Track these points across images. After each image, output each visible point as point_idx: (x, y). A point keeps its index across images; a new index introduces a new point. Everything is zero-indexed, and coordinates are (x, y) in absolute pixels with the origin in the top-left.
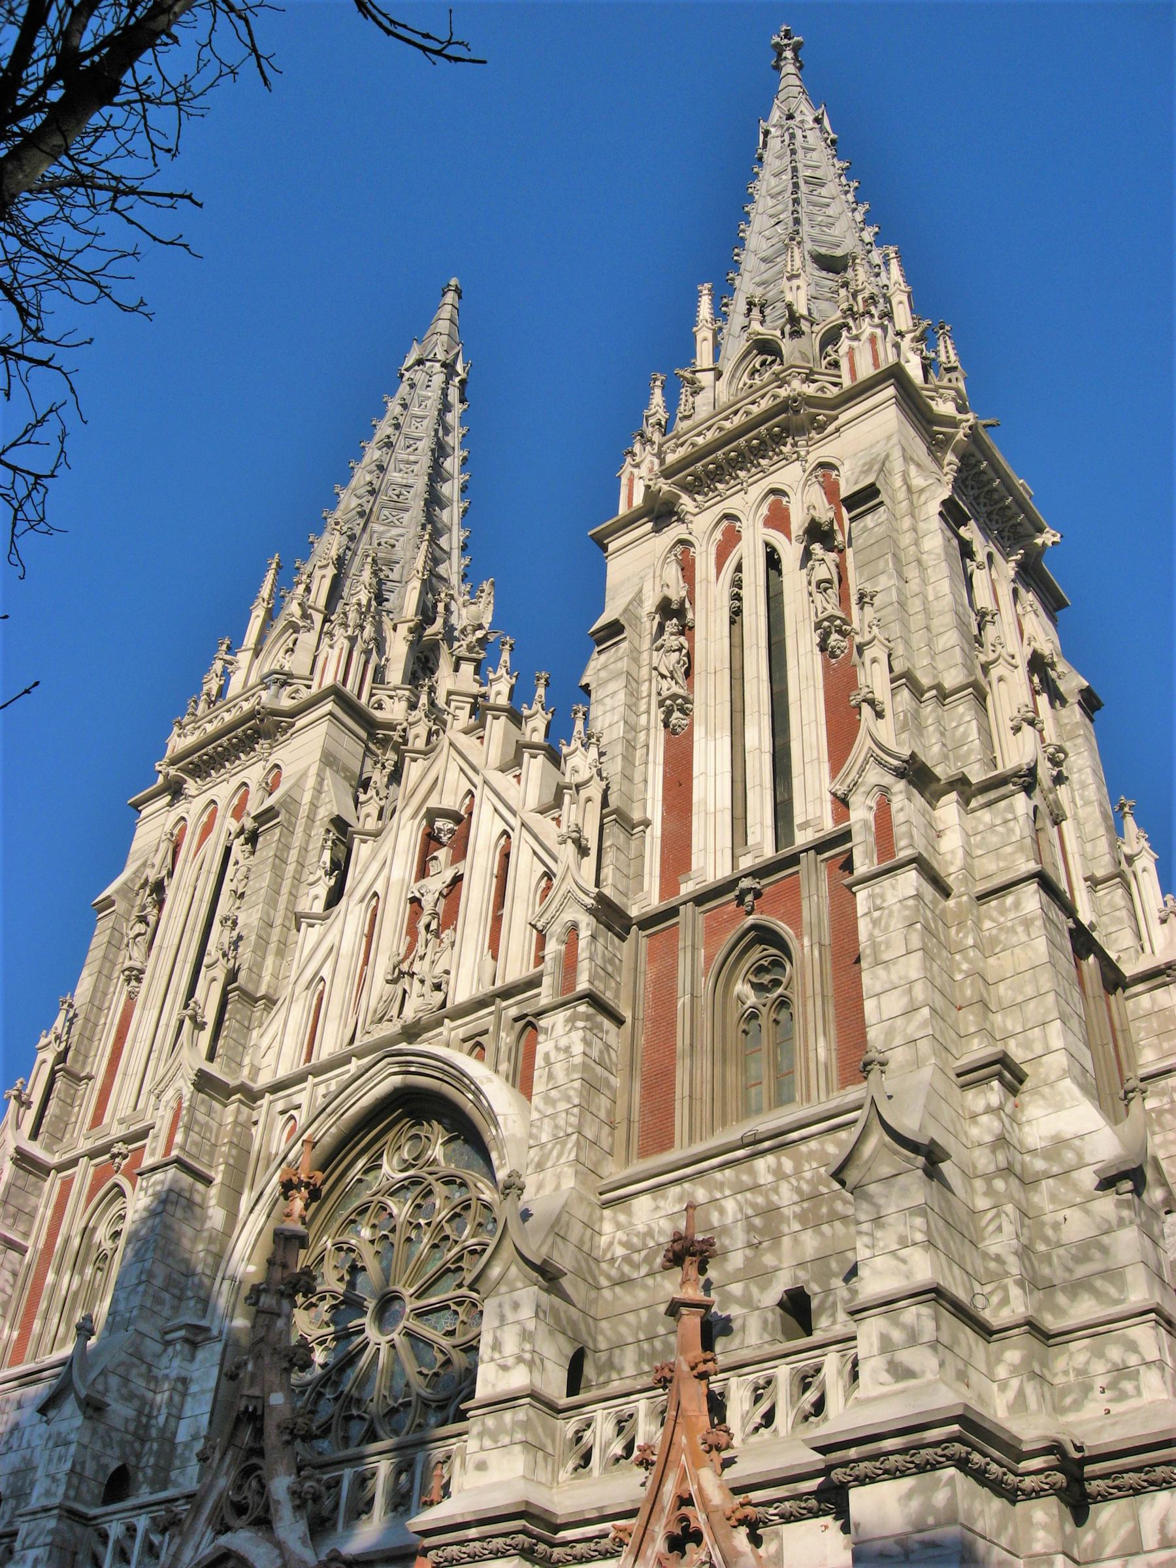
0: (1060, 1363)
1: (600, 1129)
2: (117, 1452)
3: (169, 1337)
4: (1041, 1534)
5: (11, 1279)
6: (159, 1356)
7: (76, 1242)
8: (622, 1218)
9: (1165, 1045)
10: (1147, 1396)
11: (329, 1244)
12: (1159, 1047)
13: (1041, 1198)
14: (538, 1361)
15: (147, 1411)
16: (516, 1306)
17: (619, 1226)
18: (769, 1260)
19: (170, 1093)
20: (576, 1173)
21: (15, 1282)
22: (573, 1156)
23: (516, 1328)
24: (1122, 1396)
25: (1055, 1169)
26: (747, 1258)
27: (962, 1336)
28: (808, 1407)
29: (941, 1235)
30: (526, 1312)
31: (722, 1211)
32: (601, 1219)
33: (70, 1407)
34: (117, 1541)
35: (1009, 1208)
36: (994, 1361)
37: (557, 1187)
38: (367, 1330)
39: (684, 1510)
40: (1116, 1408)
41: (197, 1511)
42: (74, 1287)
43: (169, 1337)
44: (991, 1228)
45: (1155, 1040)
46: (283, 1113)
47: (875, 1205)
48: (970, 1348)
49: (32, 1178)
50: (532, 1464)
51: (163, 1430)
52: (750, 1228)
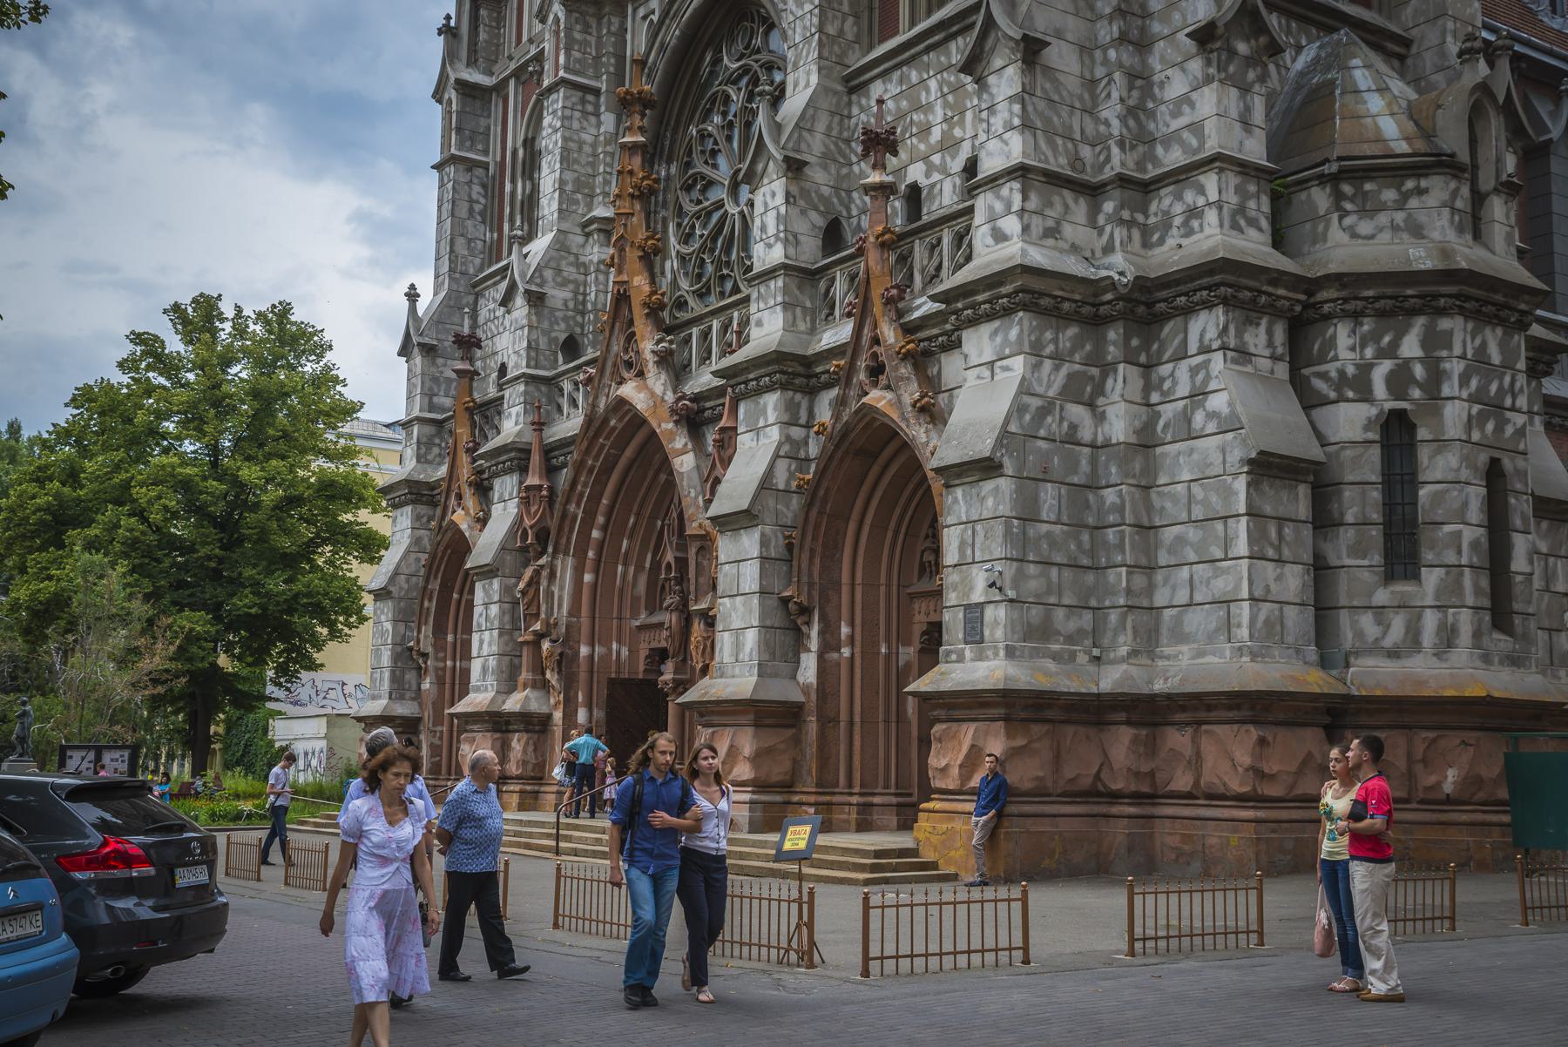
0: (1153, 207)
1: (843, 22)
2: (563, 326)
3: (587, 230)
4: (1111, 348)
5: (482, 191)
6: (583, 246)
7: (521, 152)
8: (864, 101)
10: (1207, 231)
11: (694, 132)
13: (1155, 62)
14: (791, 238)
15: (581, 290)
16: (774, 195)
17: (862, 109)
18: (957, 132)
19: (551, 17)
20: (820, 70)
21: (486, 192)
22: (816, 55)
23: (775, 212)
24: (1190, 232)
25: (1166, 32)
26: (943, 132)
27: (1056, 199)
28: (962, 260)
29: (1041, 115)
30: (780, 199)
31: (928, 91)
32: (850, 104)
33: (519, 301)
34: (570, 394)
35: (1117, 76)
36: (1094, 211)
37: (807, 85)
38: (727, 206)
39: (876, 348)
40: (1185, 242)
41: (602, 371)
42: (527, 192)
43: (587, 230)
44: (1103, 95)
46: (645, 18)
47: (991, 94)
48: (1066, 207)
49: (478, 103)
50: (790, 317)
51: (595, 304)
52: (946, 105)
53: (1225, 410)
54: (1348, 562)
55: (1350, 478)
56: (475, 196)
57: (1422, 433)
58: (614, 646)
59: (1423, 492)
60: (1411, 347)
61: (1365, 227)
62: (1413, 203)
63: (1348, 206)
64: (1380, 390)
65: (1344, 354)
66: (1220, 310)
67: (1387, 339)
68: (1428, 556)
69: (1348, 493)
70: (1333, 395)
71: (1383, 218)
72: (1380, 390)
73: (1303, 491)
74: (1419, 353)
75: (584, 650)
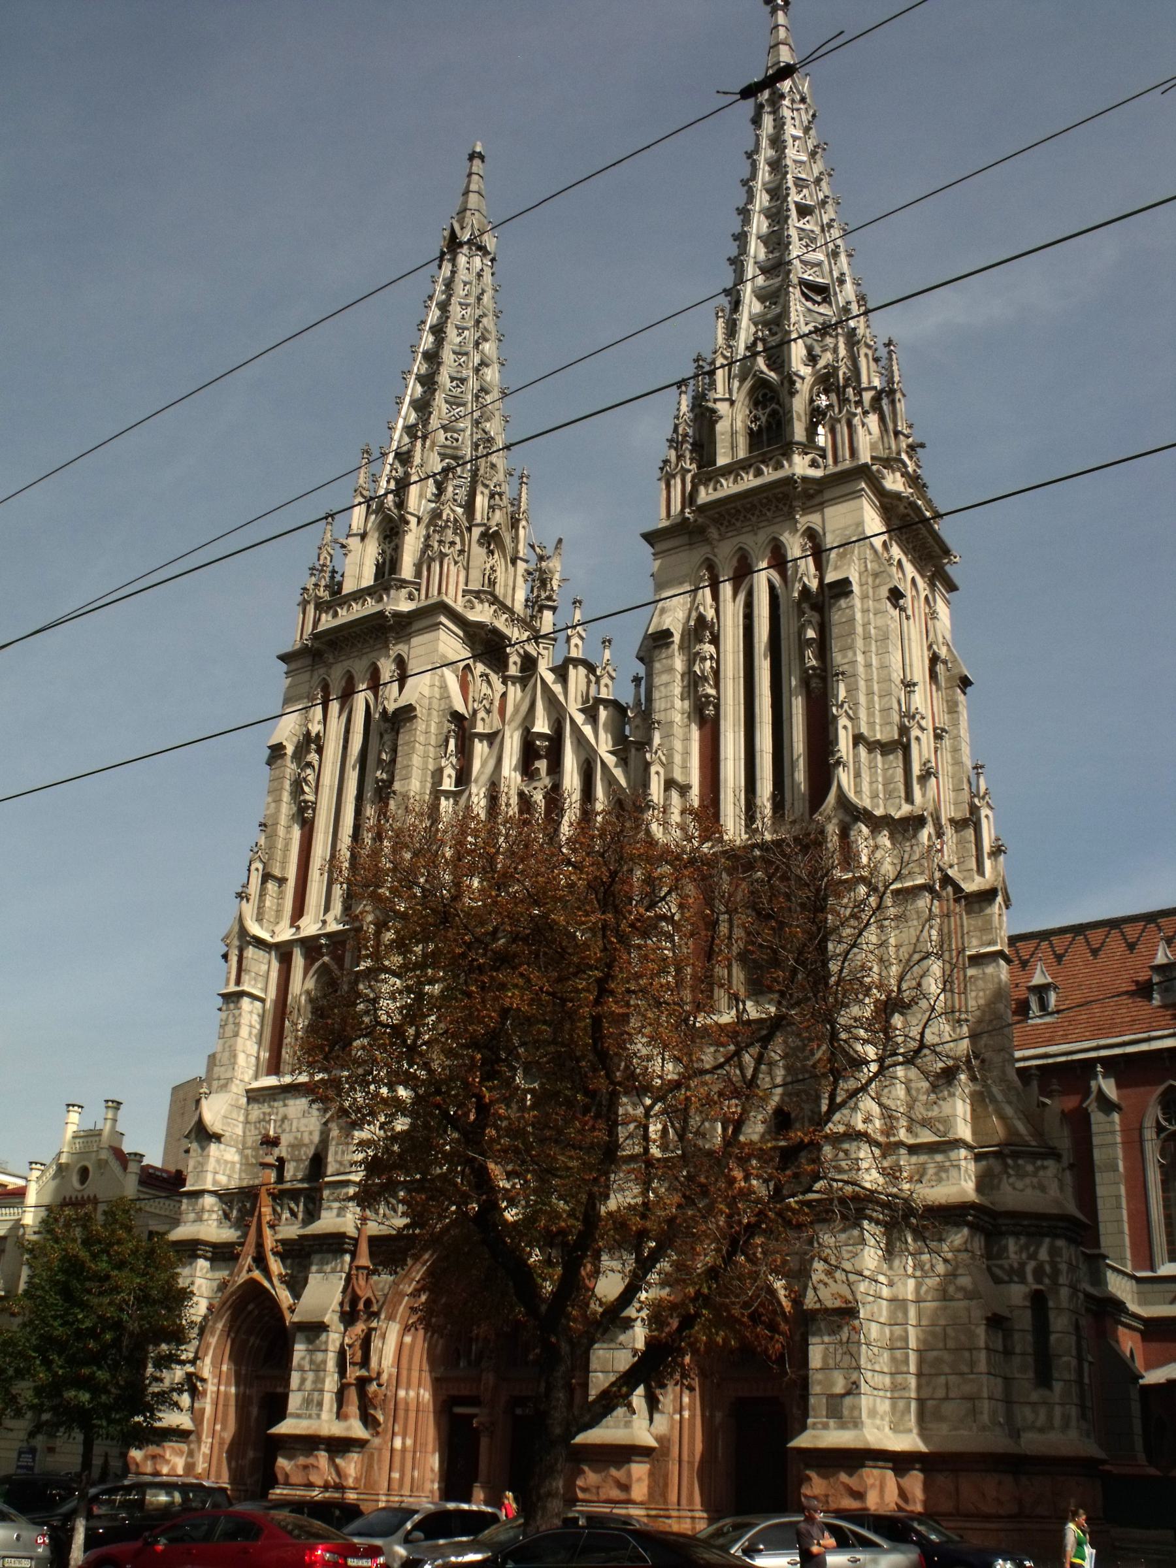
9: (984, 938)
12: (980, 938)
45: (978, 934)
53: (970, 1287)
54: (1017, 1376)
55: (1017, 1327)
56: (254, 1023)
57: (1051, 1304)
58: (422, 1391)
59: (1053, 1338)
60: (1043, 1255)
61: (1019, 1185)
62: (1041, 1173)
63: (1011, 1172)
64: (1030, 1278)
65: (1012, 1256)
66: (966, 1231)
67: (1032, 1249)
68: (1056, 1375)
69: (1017, 1336)
70: (1006, 1278)
71: (1027, 1181)
72: (1030, 1278)
73: (1000, 1335)
74: (1047, 1258)
75: (402, 1393)
